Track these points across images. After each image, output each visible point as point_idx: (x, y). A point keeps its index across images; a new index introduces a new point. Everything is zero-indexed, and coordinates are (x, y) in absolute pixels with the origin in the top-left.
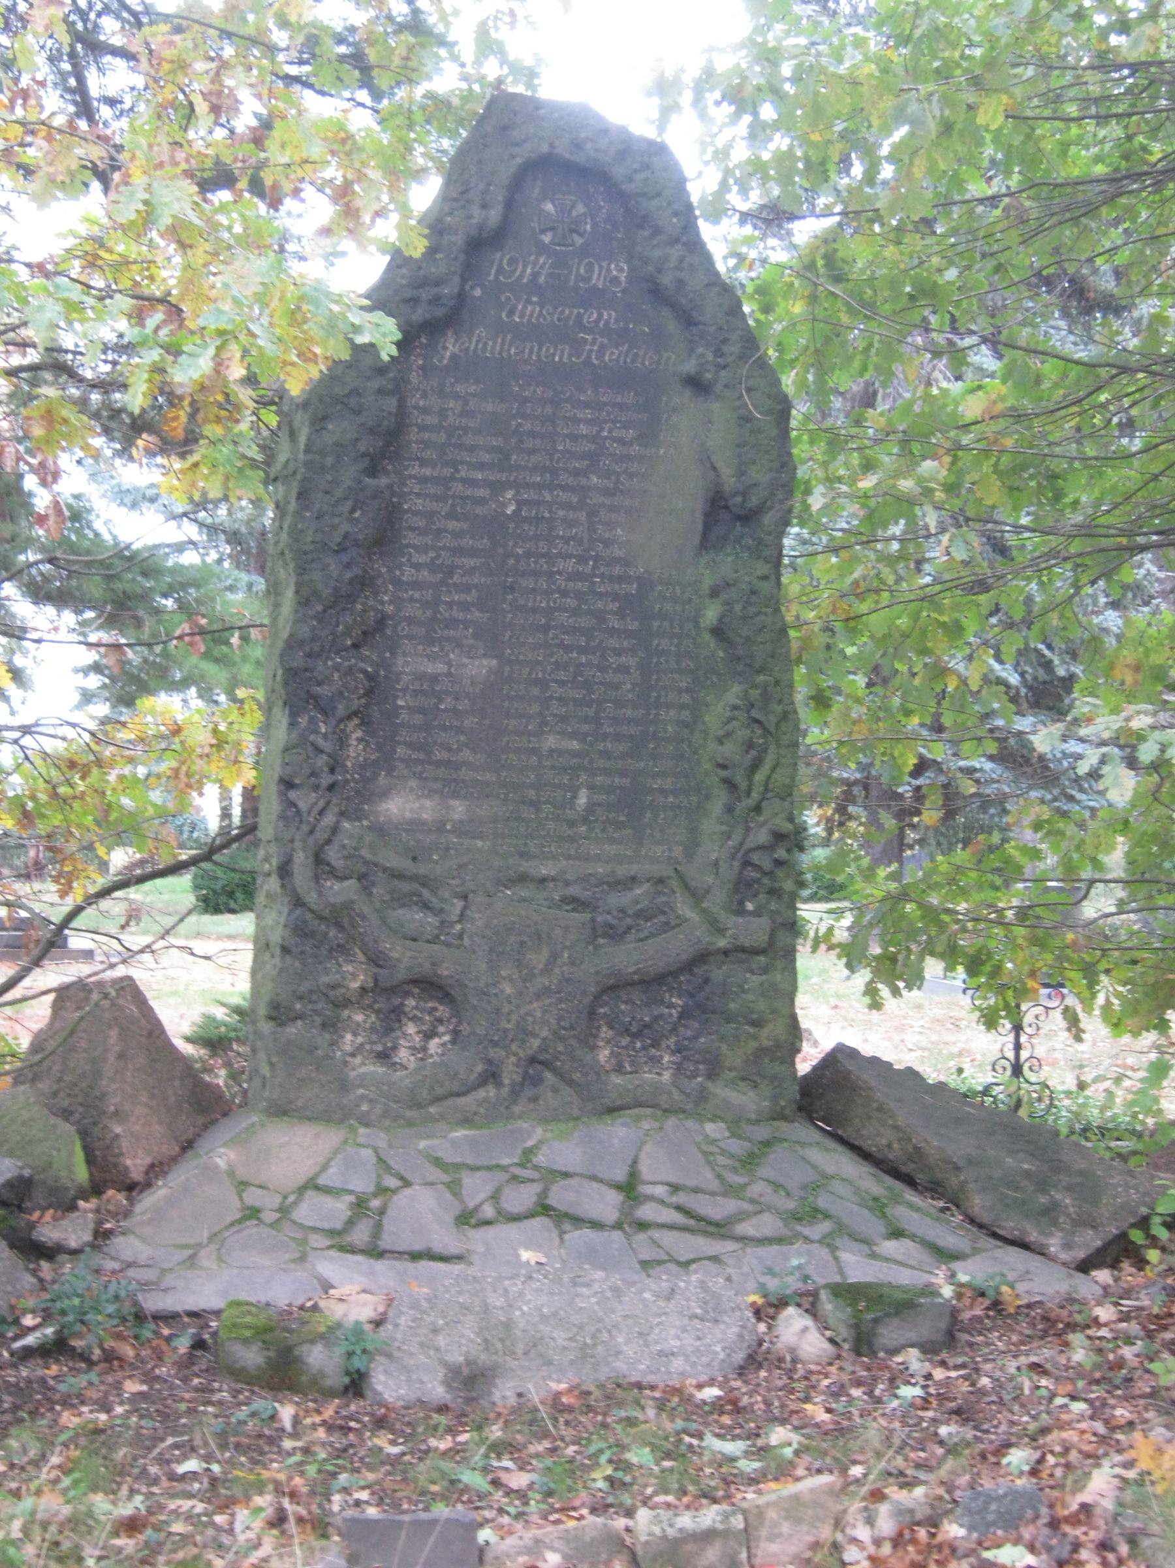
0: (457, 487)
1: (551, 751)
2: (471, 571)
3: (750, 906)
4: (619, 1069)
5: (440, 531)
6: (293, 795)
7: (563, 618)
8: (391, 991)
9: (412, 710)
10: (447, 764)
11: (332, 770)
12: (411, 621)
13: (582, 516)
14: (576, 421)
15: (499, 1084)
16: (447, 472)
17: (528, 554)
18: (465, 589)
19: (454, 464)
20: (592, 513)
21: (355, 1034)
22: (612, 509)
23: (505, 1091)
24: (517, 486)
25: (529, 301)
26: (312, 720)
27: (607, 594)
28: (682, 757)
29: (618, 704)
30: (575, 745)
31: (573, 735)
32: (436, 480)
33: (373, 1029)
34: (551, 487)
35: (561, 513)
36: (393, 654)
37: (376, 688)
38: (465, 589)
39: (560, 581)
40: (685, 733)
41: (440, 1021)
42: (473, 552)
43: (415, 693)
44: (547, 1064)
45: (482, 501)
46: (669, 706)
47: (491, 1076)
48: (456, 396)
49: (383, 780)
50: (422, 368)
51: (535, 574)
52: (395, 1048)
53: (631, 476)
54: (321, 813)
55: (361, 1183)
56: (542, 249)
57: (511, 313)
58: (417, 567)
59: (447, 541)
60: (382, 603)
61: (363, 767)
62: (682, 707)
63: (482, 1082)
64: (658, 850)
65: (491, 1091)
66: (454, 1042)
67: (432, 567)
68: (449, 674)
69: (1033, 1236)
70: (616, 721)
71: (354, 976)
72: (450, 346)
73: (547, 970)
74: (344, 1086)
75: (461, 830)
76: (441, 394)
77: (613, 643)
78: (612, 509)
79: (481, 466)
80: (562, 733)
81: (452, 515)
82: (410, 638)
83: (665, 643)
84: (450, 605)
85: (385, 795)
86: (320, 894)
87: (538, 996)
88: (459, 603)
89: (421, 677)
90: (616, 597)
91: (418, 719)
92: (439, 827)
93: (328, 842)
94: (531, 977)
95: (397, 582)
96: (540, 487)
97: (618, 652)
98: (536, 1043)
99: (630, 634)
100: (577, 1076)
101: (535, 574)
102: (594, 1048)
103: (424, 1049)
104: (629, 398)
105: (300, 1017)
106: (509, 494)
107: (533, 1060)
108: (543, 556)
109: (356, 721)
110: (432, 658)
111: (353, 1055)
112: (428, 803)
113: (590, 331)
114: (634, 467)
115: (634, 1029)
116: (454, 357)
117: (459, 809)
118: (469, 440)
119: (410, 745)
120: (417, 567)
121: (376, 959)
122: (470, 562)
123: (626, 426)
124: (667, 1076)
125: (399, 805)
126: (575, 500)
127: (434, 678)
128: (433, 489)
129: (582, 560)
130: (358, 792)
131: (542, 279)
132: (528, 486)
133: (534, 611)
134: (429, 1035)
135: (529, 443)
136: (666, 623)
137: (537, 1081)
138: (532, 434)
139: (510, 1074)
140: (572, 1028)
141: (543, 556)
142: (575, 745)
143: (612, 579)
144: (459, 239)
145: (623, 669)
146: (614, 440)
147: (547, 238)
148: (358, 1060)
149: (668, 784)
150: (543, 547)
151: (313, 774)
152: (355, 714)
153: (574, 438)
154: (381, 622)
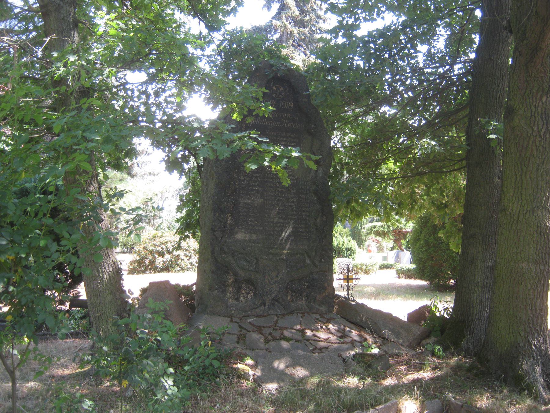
3: (323, 260)
4: (293, 301)
6: (215, 233)
7: (278, 189)
21: (230, 294)
26: (220, 214)
41: (251, 290)
44: (277, 301)
49: (236, 229)
51: (272, 178)
52: (240, 297)
58: (244, 176)
63: (261, 305)
65: (263, 307)
66: (254, 295)
71: (230, 279)
73: (277, 276)
74: (227, 307)
77: (290, 195)
84: (252, 185)
85: (237, 233)
87: (274, 283)
92: (250, 241)
98: (274, 295)
100: (283, 303)
101: (272, 178)
103: (247, 297)
105: (216, 289)
107: (273, 299)
110: (248, 199)
111: (229, 299)
112: (247, 235)
117: (254, 237)
120: (244, 176)
121: (235, 274)
124: (304, 302)
125: (240, 236)
133: (272, 187)
137: (273, 304)
139: (268, 303)
145: (293, 202)
147: (274, 96)
148: (231, 300)
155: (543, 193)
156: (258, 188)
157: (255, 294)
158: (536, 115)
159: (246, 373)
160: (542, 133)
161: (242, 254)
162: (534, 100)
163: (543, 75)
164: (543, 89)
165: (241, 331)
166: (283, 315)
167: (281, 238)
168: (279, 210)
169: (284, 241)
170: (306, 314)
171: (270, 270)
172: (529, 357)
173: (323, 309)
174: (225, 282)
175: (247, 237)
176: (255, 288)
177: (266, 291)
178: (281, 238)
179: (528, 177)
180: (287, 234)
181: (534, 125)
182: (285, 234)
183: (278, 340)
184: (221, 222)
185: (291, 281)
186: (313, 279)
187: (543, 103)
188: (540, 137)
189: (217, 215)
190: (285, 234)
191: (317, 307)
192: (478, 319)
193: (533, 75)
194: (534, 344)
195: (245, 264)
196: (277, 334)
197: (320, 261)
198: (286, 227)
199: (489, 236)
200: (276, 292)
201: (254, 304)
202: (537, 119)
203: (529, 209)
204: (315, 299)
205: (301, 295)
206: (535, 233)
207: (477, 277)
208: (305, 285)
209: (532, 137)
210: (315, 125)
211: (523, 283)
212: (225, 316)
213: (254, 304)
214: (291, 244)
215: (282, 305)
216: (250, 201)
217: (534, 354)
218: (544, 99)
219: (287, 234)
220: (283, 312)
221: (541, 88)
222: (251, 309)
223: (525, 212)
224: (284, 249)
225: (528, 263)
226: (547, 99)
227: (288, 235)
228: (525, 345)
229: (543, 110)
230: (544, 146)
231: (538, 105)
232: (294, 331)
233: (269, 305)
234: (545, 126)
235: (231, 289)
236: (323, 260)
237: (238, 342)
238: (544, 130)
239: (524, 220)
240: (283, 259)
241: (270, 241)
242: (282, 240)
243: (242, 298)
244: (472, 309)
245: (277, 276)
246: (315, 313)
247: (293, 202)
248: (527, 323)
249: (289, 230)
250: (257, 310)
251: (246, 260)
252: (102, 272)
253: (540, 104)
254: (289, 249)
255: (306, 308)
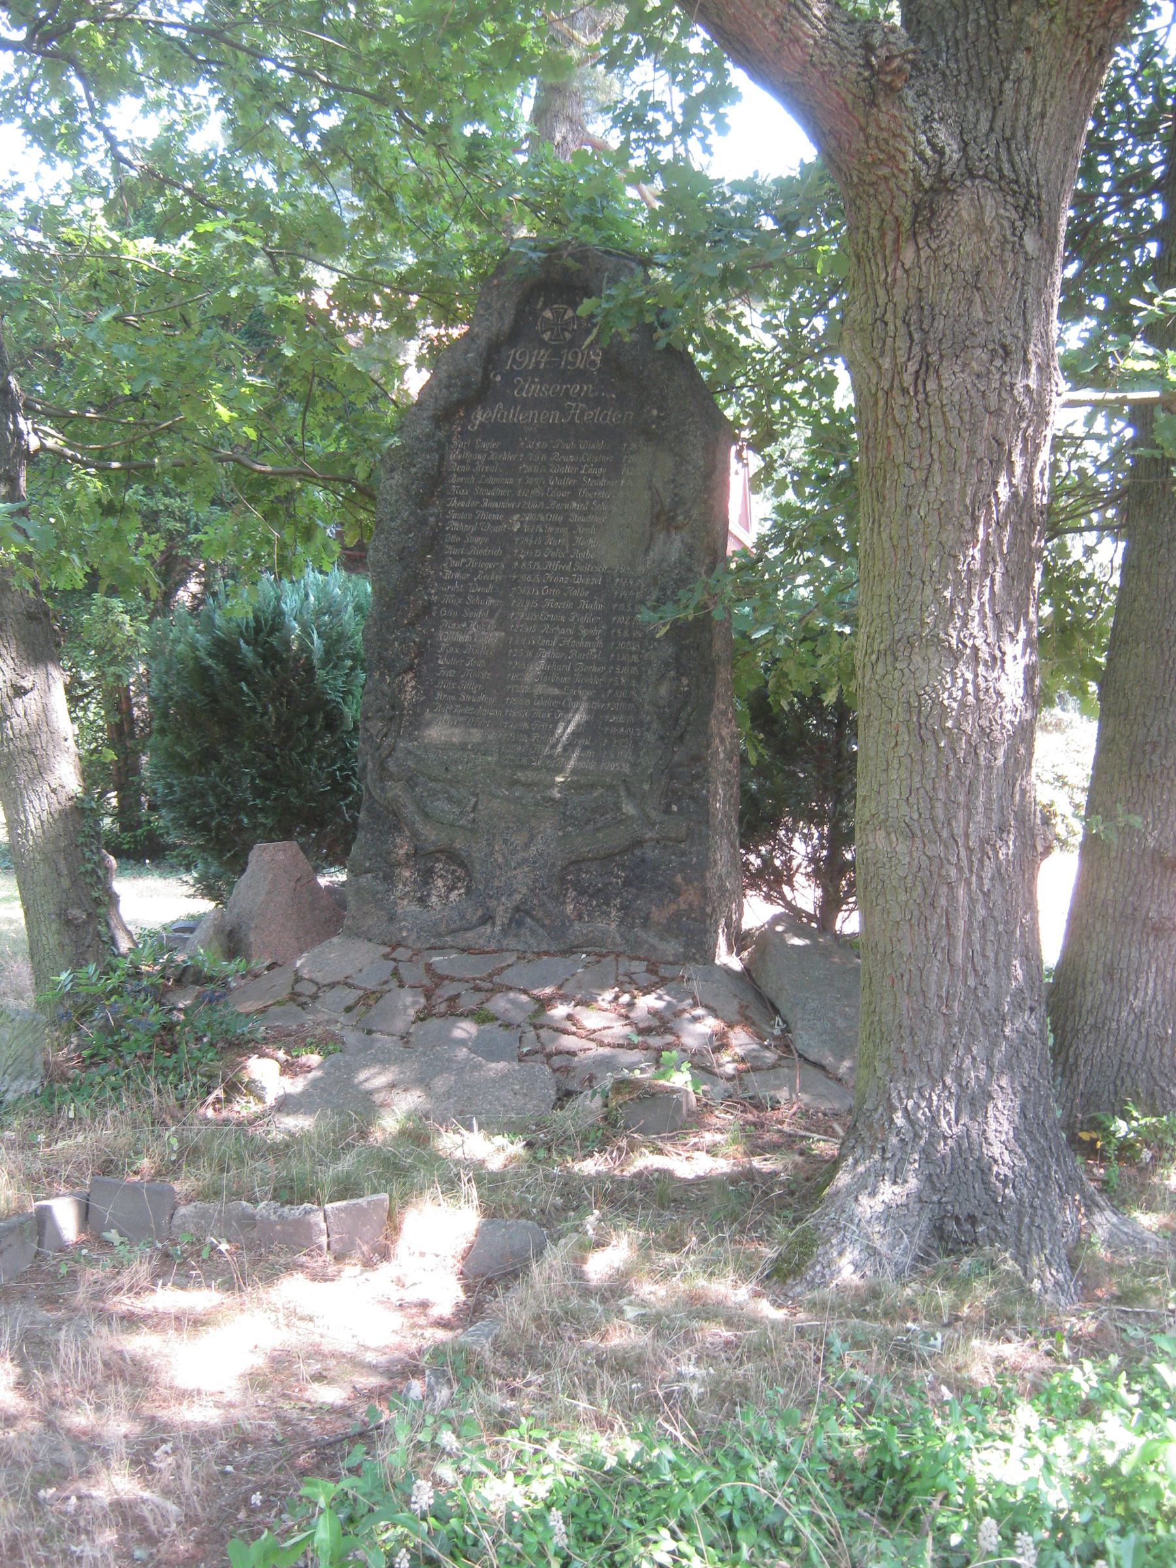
0: (483, 515)
1: (539, 696)
2: (489, 572)
3: (675, 808)
5: (469, 545)
7: (549, 603)
8: (429, 855)
9: (449, 667)
10: (470, 704)
11: (393, 708)
12: (448, 606)
13: (565, 530)
14: (563, 464)
15: (494, 924)
16: (474, 504)
17: (527, 559)
18: (485, 584)
19: (480, 498)
20: (572, 527)
21: (405, 885)
22: (585, 525)
23: (498, 929)
24: (520, 511)
25: (533, 382)
26: (382, 675)
27: (582, 585)
28: (630, 700)
29: (588, 662)
30: (556, 691)
31: (555, 685)
32: (468, 510)
33: (415, 882)
34: (544, 512)
35: (551, 529)
36: (437, 629)
37: (426, 651)
38: (485, 584)
39: (549, 577)
40: (634, 683)
42: (491, 558)
43: (449, 657)
44: (528, 913)
45: (494, 523)
46: (623, 664)
47: (488, 919)
48: (482, 451)
49: (428, 715)
50: (460, 433)
51: (531, 572)
52: (429, 895)
53: (600, 501)
54: (385, 735)
55: (371, 985)
56: (543, 344)
57: (521, 390)
58: (454, 570)
59: (475, 551)
60: (429, 595)
61: (415, 706)
62: (633, 664)
64: (612, 766)
65: (488, 929)
67: (463, 570)
68: (473, 643)
69: (829, 1060)
70: (586, 674)
72: (480, 416)
74: (392, 919)
75: (476, 749)
76: (472, 449)
77: (585, 619)
78: (585, 525)
79: (498, 499)
80: (549, 684)
81: (478, 533)
82: (448, 618)
83: (621, 619)
84: (475, 594)
85: (428, 724)
86: (383, 789)
87: (519, 865)
88: (480, 594)
89: (453, 644)
90: (588, 588)
91: (451, 673)
92: (463, 747)
93: (390, 755)
94: (513, 852)
95: (440, 580)
96: (538, 511)
97: (587, 626)
98: (518, 897)
99: (597, 613)
100: (547, 922)
102: (564, 903)
103: (447, 897)
104: (599, 445)
105: (367, 871)
106: (516, 517)
107: (517, 909)
108: (537, 559)
109: (411, 675)
110: (464, 631)
113: (575, 400)
114: (602, 494)
115: (591, 891)
116: (481, 424)
117: (476, 735)
118: (491, 480)
119: (445, 691)
120: (454, 570)
121: (415, 835)
122: (490, 565)
123: (598, 465)
124: (613, 925)
126: (560, 519)
127: (462, 646)
128: (463, 516)
129: (564, 561)
130: (411, 723)
131: (542, 366)
132: (527, 511)
134: (451, 889)
135: (530, 481)
136: (622, 605)
137: (520, 924)
138: (531, 475)
139: (501, 917)
140: (544, 888)
141: (537, 559)
142: (556, 691)
143: (585, 575)
144: (482, 342)
145: (592, 638)
146: (589, 476)
147: (546, 337)
148: (405, 902)
149: (621, 719)
150: (538, 553)
151: (380, 710)
152: (411, 668)
153: (561, 476)
154: (427, 608)
155: (928, 591)
156: (491, 601)
157: (468, 888)
158: (889, 317)
159: (254, 1081)
160: (908, 379)
161: (436, 780)
162: (881, 264)
163: (885, 171)
164: (896, 218)
165: (386, 982)
166: (539, 954)
167: (552, 741)
168: (549, 661)
169: (559, 749)
170: (611, 958)
171: (508, 828)
172: (873, 1149)
173: (671, 948)
174: (389, 853)
175: (456, 735)
176: (469, 874)
177: (496, 883)
178: (552, 741)
179: (884, 536)
180: (569, 730)
181: (882, 354)
182: (566, 730)
183: (462, 1014)
184: (384, 694)
185: (575, 862)
186: (643, 860)
187: (906, 271)
188: (905, 391)
189: (377, 675)
190: (566, 730)
191: (655, 941)
192: (1094, 1026)
193: (855, 179)
194: (906, 1109)
195: (447, 807)
196: (469, 1001)
197: (667, 811)
198: (567, 711)
199: (1155, 745)
200: (524, 890)
201: (463, 917)
202: (891, 327)
203: (882, 647)
204: (647, 918)
205: (608, 905)
206: (903, 729)
207: (1104, 884)
208: (618, 877)
209: (880, 394)
210: (660, 409)
211: (881, 901)
212: (384, 944)
213: (463, 917)
214: (579, 759)
215: (543, 926)
216: (467, 638)
217: (894, 1140)
218: (908, 255)
219: (569, 730)
220: (545, 947)
221: (889, 218)
222: (454, 931)
223: (874, 657)
224: (559, 771)
225: (888, 834)
226: (919, 256)
227: (573, 733)
228: (876, 1109)
229: (912, 294)
230: (924, 424)
231: (895, 280)
232: (524, 998)
233: (503, 925)
234: (916, 349)
235: (407, 874)
236: (675, 808)
237: (349, 1009)
238: (912, 367)
239: (873, 685)
240: (551, 799)
241: (519, 749)
242: (554, 746)
243: (434, 899)
244: (1079, 991)
245: (527, 846)
246: (639, 959)
247: (592, 638)
248: (895, 1037)
249: (577, 718)
250: (469, 934)
251: (450, 799)
252: (25, 811)
253: (899, 272)
254: (574, 772)
255: (618, 940)
